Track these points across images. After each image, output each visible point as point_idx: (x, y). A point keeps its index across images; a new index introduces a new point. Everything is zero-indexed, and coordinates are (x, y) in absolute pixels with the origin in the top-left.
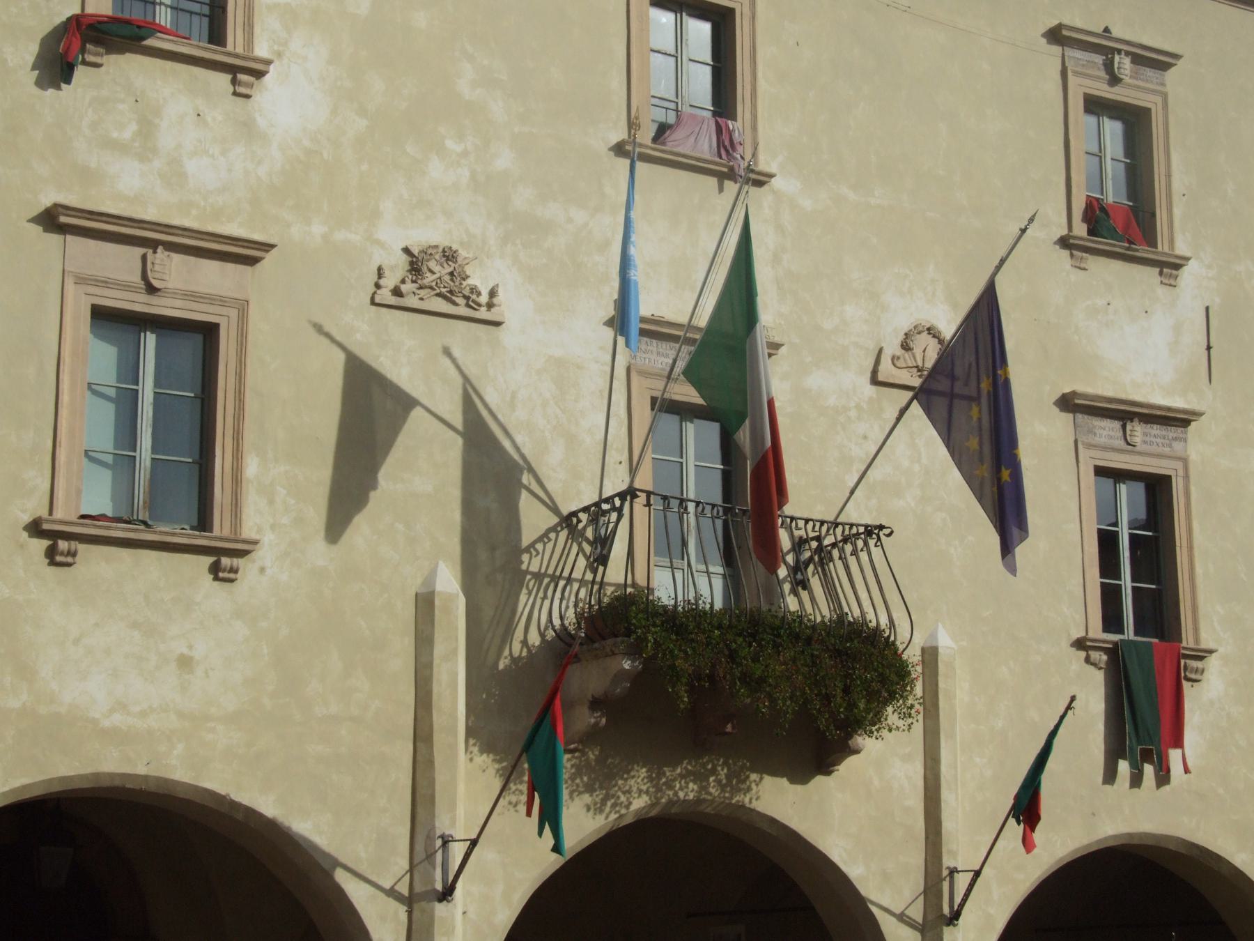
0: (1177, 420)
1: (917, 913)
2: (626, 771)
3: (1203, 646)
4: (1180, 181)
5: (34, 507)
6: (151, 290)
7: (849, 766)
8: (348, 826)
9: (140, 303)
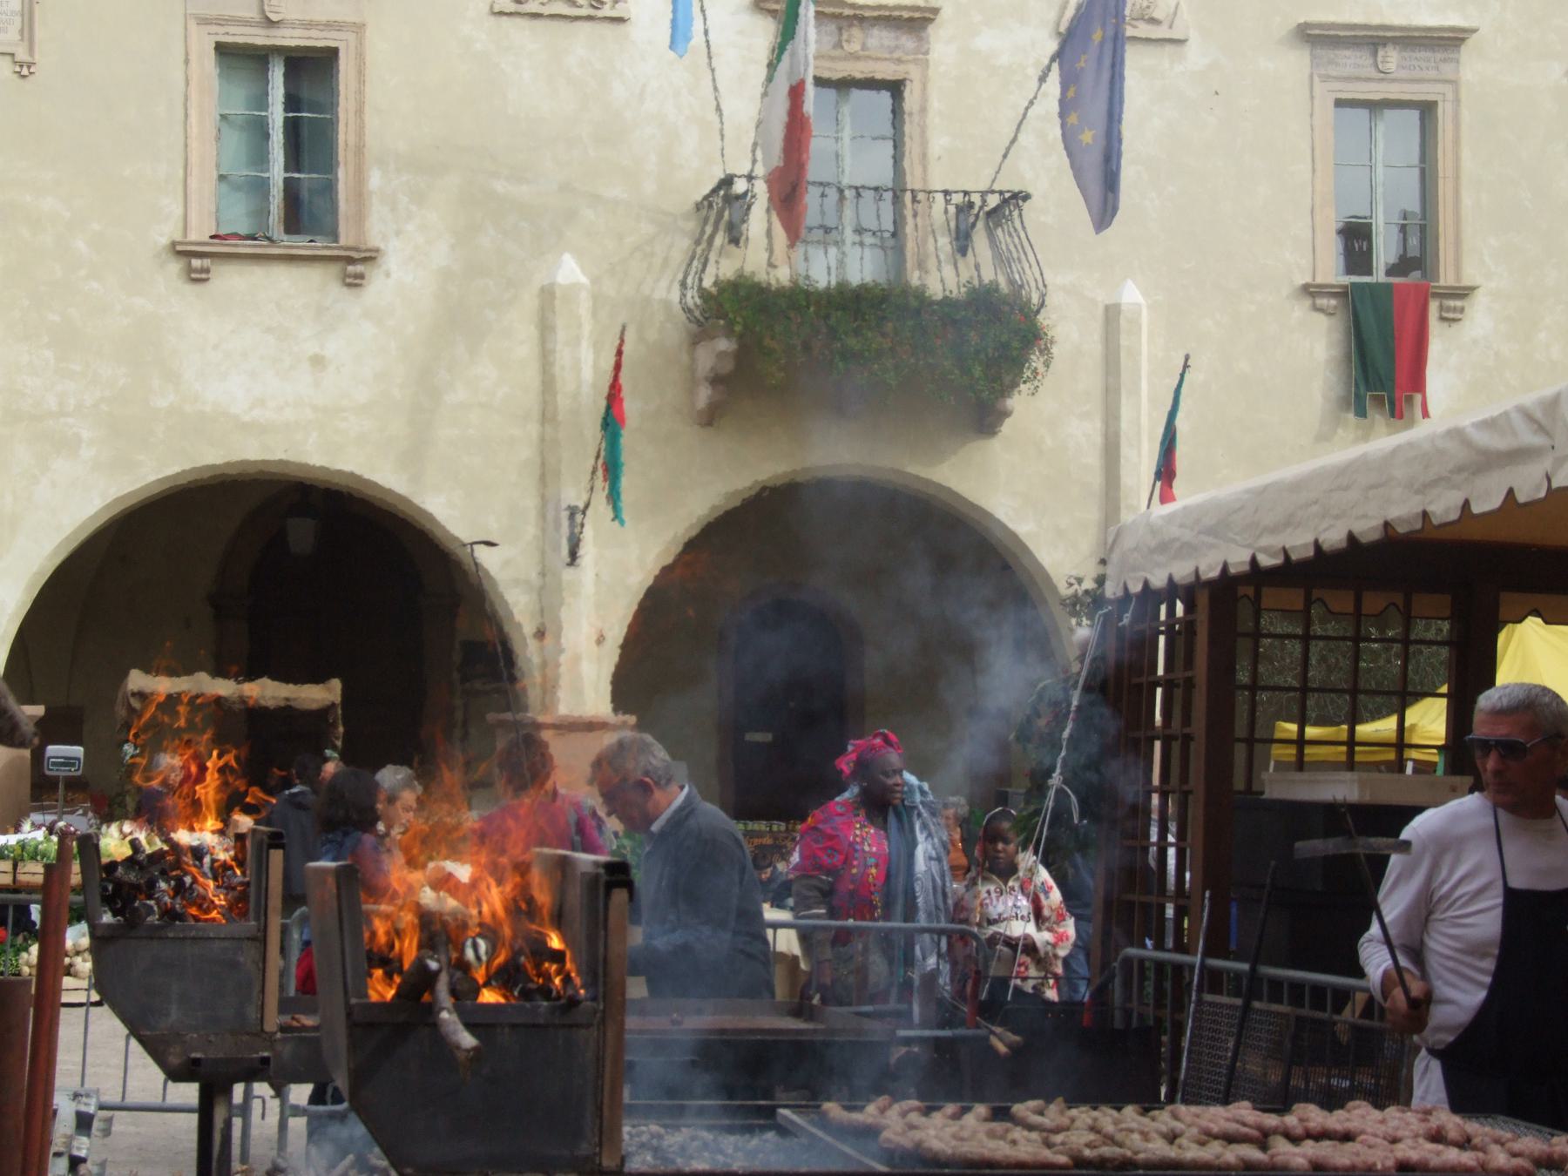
3: (1466, 282)
6: (270, 23)
7: (1007, 427)
8: (472, 500)
9: (260, 38)
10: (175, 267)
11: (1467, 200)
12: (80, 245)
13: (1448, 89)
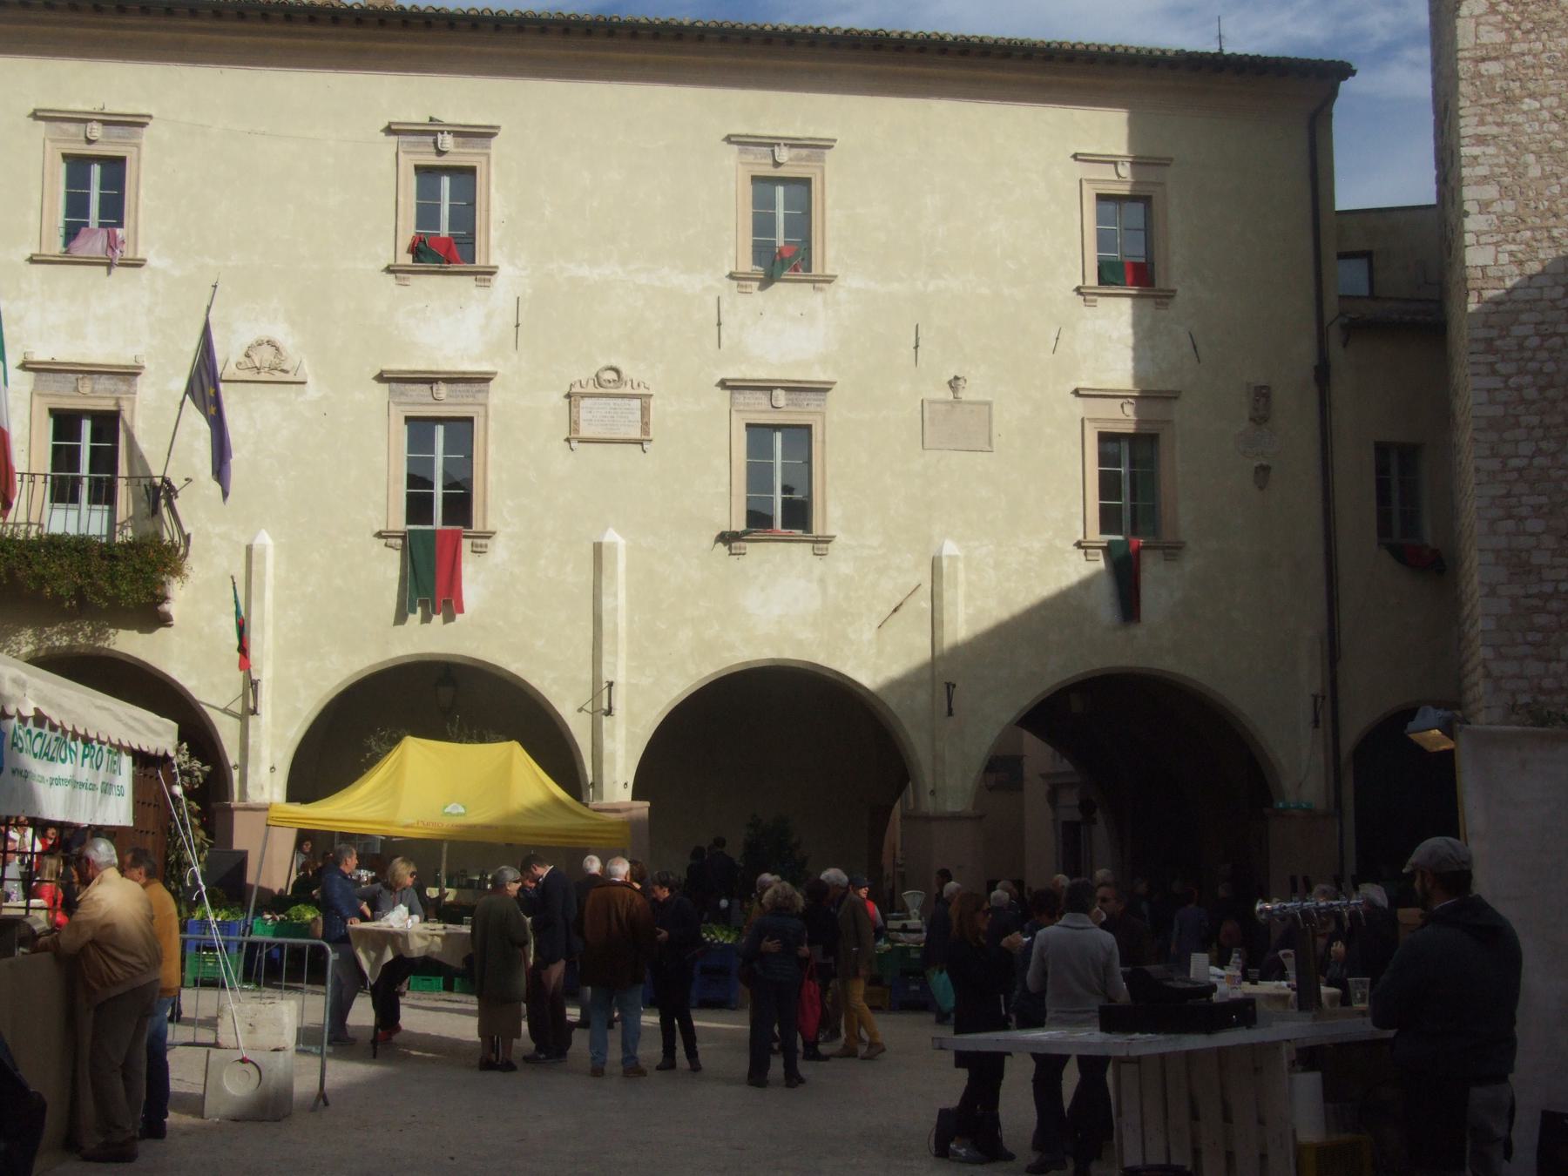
0: (484, 379)
1: (237, 708)
2: (16, 631)
3: (489, 528)
4: (496, 214)
11: (491, 477)
13: (481, 410)
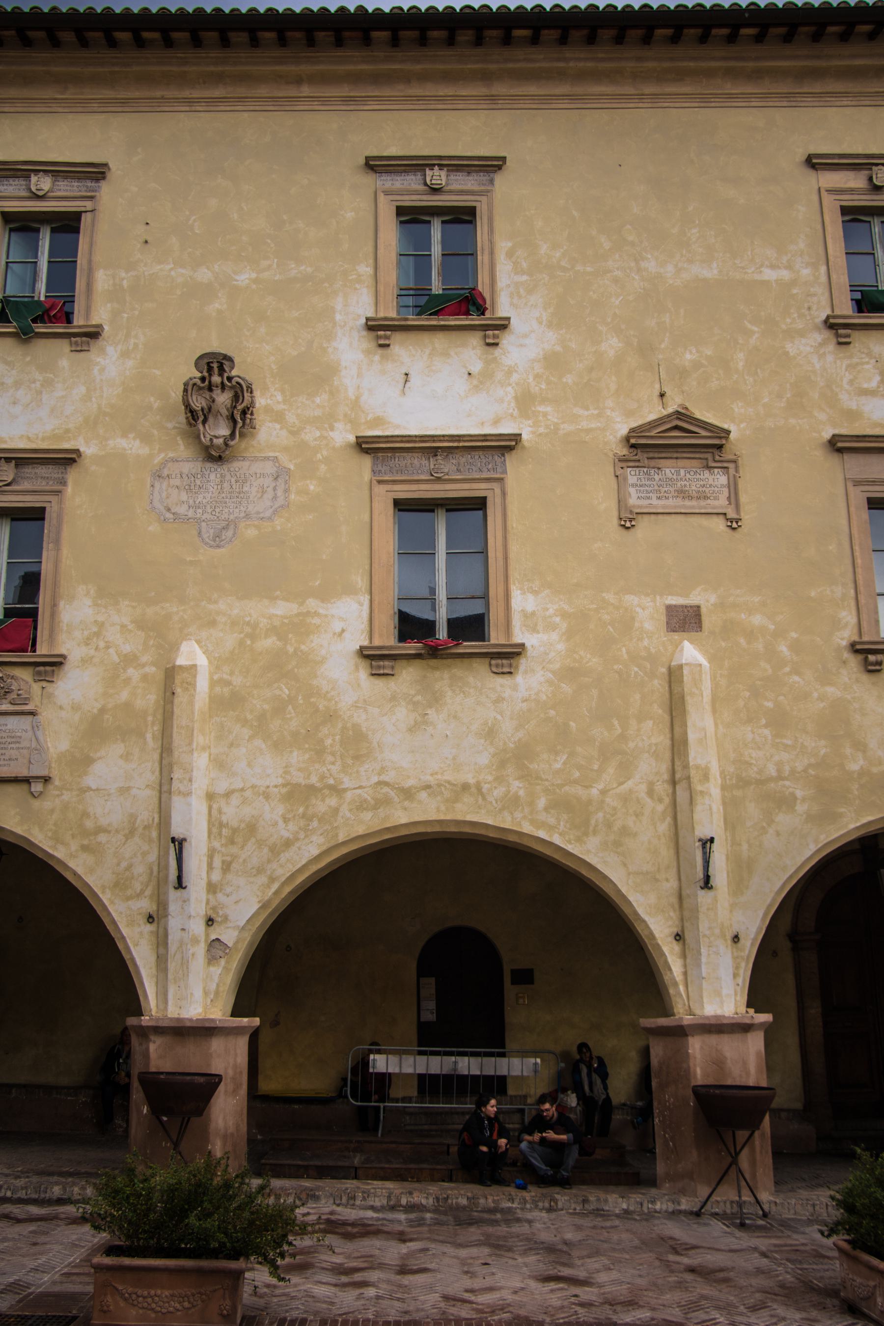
5: (846, 635)
10: (854, 662)
12: (783, 649)
